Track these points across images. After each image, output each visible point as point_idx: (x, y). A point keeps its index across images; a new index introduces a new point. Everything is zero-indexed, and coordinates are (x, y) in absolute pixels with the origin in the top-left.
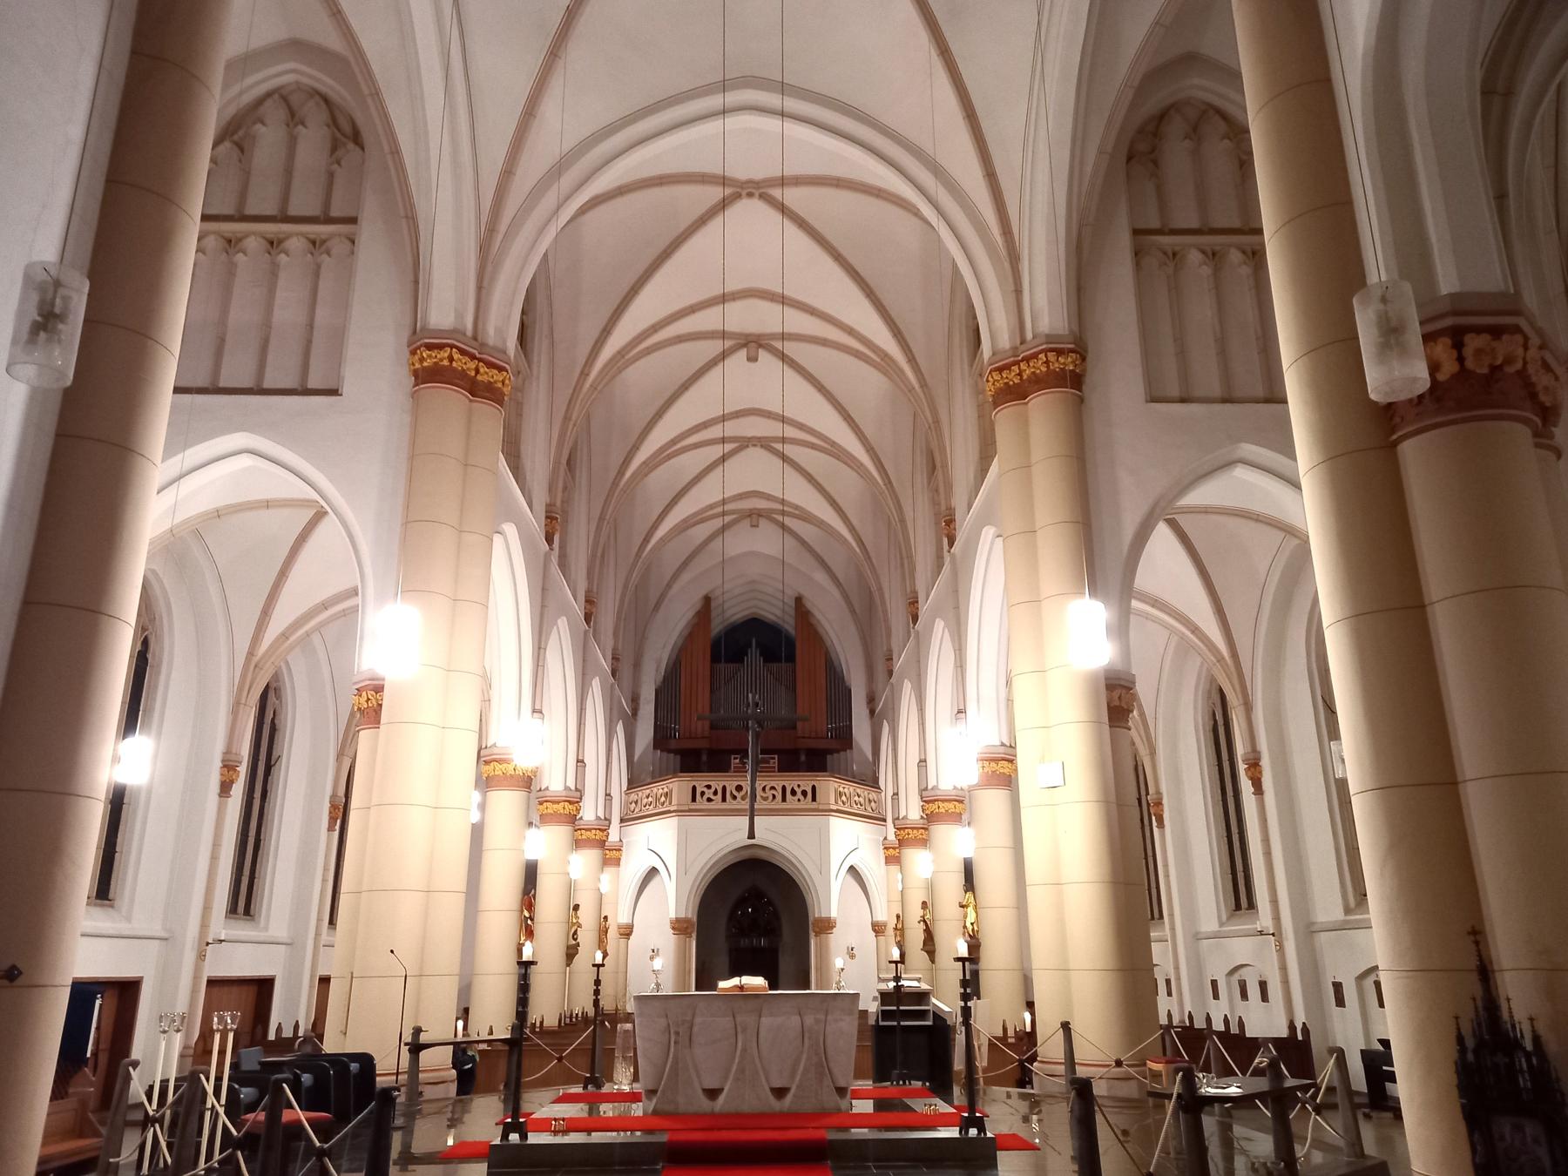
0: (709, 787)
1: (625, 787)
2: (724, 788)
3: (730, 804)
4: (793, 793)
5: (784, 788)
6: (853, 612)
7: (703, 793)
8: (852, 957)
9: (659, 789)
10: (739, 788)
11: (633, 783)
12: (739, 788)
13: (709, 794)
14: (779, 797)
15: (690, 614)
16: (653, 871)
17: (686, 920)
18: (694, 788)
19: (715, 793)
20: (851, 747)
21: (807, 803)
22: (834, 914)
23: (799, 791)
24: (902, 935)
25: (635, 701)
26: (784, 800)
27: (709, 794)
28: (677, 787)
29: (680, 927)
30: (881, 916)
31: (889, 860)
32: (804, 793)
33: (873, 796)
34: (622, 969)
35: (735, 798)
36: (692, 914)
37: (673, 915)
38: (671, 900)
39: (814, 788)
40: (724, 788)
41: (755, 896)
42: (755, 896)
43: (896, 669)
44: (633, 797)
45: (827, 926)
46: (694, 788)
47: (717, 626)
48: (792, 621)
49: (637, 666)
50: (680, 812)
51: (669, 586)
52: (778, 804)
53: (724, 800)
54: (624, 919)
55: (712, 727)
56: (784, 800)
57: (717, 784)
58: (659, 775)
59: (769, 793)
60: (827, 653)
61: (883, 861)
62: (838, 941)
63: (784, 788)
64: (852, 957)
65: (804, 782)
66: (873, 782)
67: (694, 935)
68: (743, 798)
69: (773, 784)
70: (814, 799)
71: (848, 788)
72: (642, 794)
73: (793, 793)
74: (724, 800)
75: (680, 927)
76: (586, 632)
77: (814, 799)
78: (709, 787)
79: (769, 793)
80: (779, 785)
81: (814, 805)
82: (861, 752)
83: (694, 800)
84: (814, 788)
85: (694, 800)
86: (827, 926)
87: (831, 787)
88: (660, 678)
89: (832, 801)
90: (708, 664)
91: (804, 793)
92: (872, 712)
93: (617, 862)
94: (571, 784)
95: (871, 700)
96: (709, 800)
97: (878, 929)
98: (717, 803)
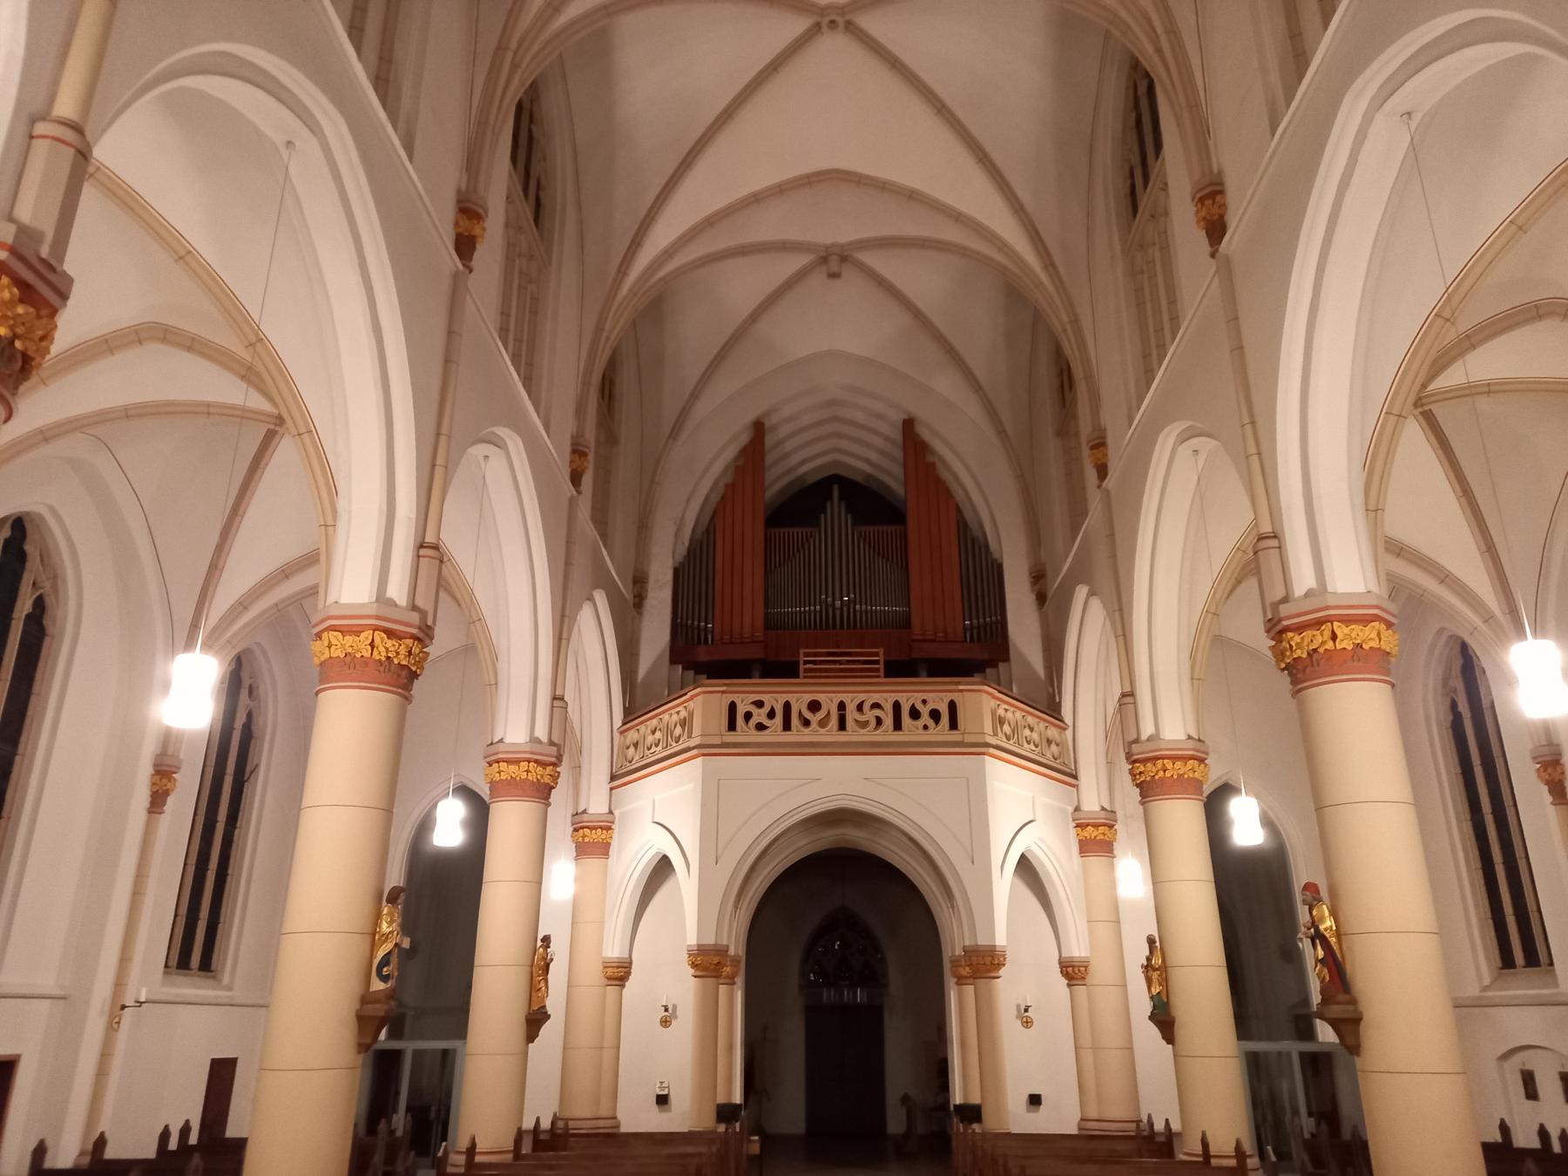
0: (759, 704)
1: (618, 721)
2: (787, 707)
3: (798, 734)
4: (915, 714)
5: (897, 707)
6: (1001, 432)
7: (748, 716)
8: (1027, 1023)
9: (671, 715)
10: (814, 706)
11: (632, 712)
12: (814, 706)
13: (759, 716)
14: (888, 721)
15: (730, 453)
16: (662, 868)
17: (721, 951)
18: (732, 708)
19: (771, 715)
20: (1007, 659)
21: (941, 732)
22: (1001, 940)
23: (925, 711)
24: (1165, 982)
25: (640, 582)
26: (898, 726)
27: (759, 716)
28: (702, 705)
29: (707, 962)
30: (1077, 949)
31: (1085, 847)
32: (935, 715)
33: (1053, 733)
34: (609, 1041)
35: (806, 723)
36: (736, 947)
37: (692, 939)
38: (691, 914)
39: (952, 706)
40: (787, 707)
41: (841, 924)
42: (841, 924)
43: (1050, 594)
44: (632, 736)
45: (985, 963)
46: (732, 708)
47: (777, 479)
48: (898, 471)
49: (643, 527)
50: (707, 749)
51: (695, 396)
52: (887, 734)
53: (787, 726)
54: (614, 950)
55: (768, 626)
56: (898, 726)
57: (774, 700)
58: (675, 691)
59: (870, 715)
60: (962, 525)
61: (1075, 849)
62: (1009, 989)
63: (897, 707)
64: (1027, 1023)
65: (933, 694)
66: (1052, 709)
67: (740, 981)
68: (823, 723)
69: (876, 698)
70: (953, 725)
71: (1014, 713)
72: (645, 729)
73: (915, 714)
74: (787, 726)
75: (707, 962)
76: (572, 503)
77: (953, 725)
78: (759, 704)
79: (870, 715)
80: (887, 701)
81: (954, 736)
82: (1026, 665)
83: (732, 726)
84: (952, 706)
85: (732, 726)
86: (985, 963)
87: (983, 704)
88: (682, 550)
89: (988, 728)
90: (760, 527)
91: (935, 715)
92: (1041, 598)
93: (603, 849)
94: (541, 733)
95: (1038, 577)
96: (761, 727)
97: (1073, 972)
98: (775, 732)
